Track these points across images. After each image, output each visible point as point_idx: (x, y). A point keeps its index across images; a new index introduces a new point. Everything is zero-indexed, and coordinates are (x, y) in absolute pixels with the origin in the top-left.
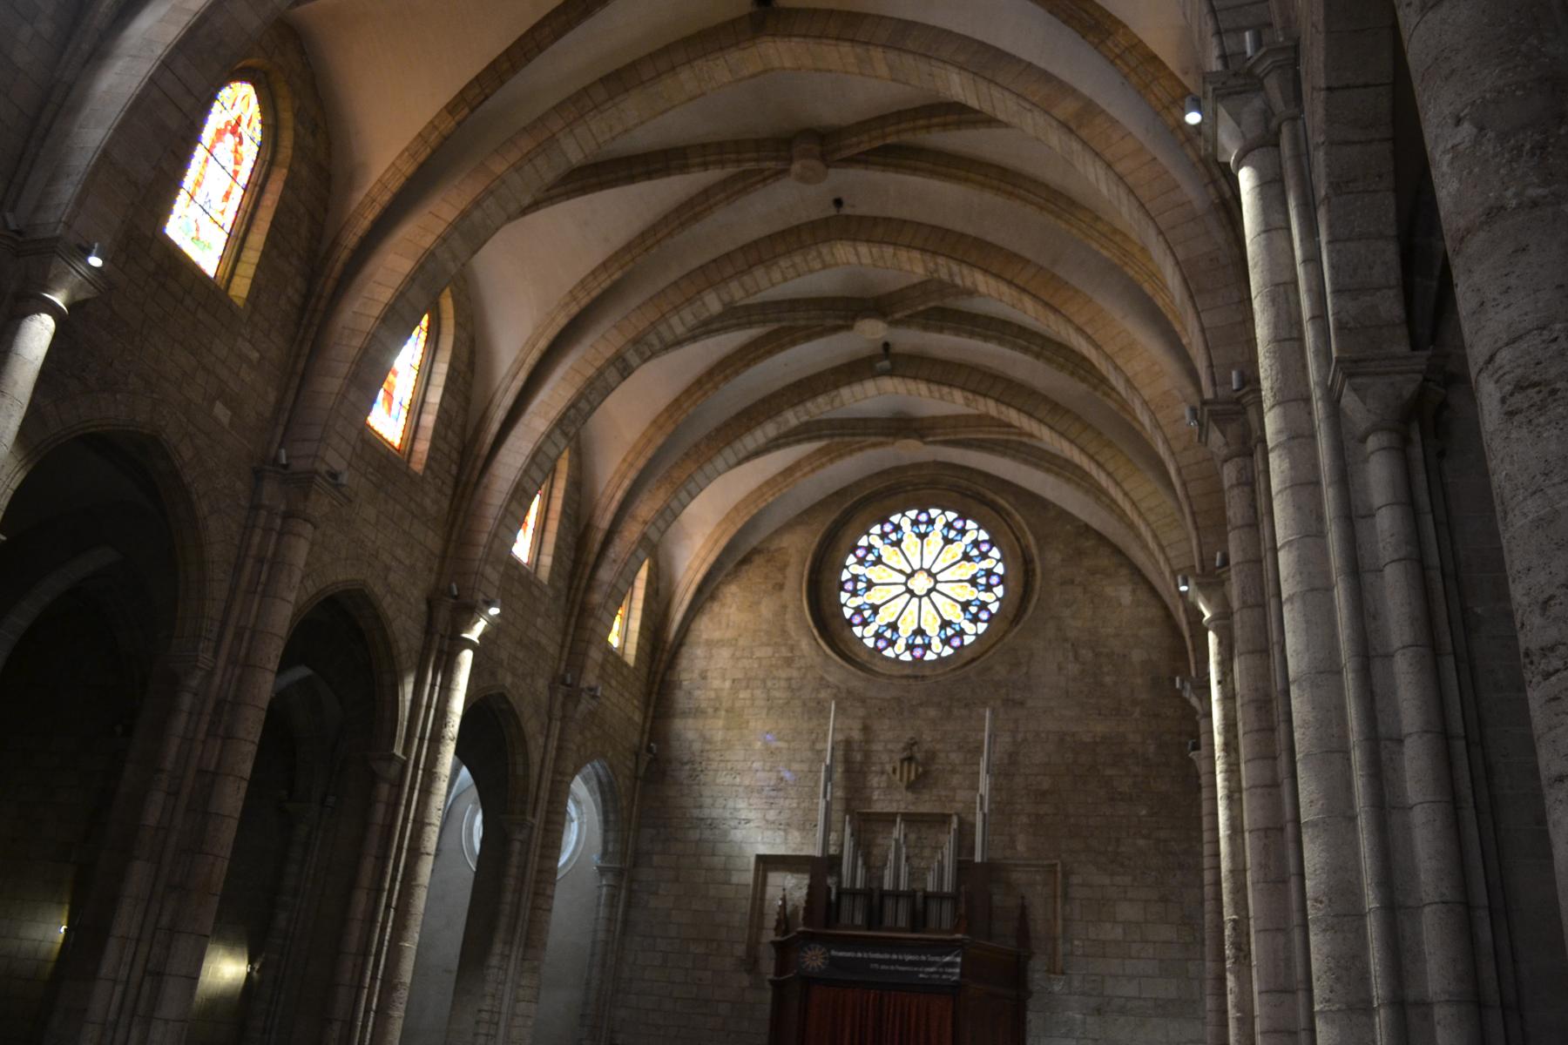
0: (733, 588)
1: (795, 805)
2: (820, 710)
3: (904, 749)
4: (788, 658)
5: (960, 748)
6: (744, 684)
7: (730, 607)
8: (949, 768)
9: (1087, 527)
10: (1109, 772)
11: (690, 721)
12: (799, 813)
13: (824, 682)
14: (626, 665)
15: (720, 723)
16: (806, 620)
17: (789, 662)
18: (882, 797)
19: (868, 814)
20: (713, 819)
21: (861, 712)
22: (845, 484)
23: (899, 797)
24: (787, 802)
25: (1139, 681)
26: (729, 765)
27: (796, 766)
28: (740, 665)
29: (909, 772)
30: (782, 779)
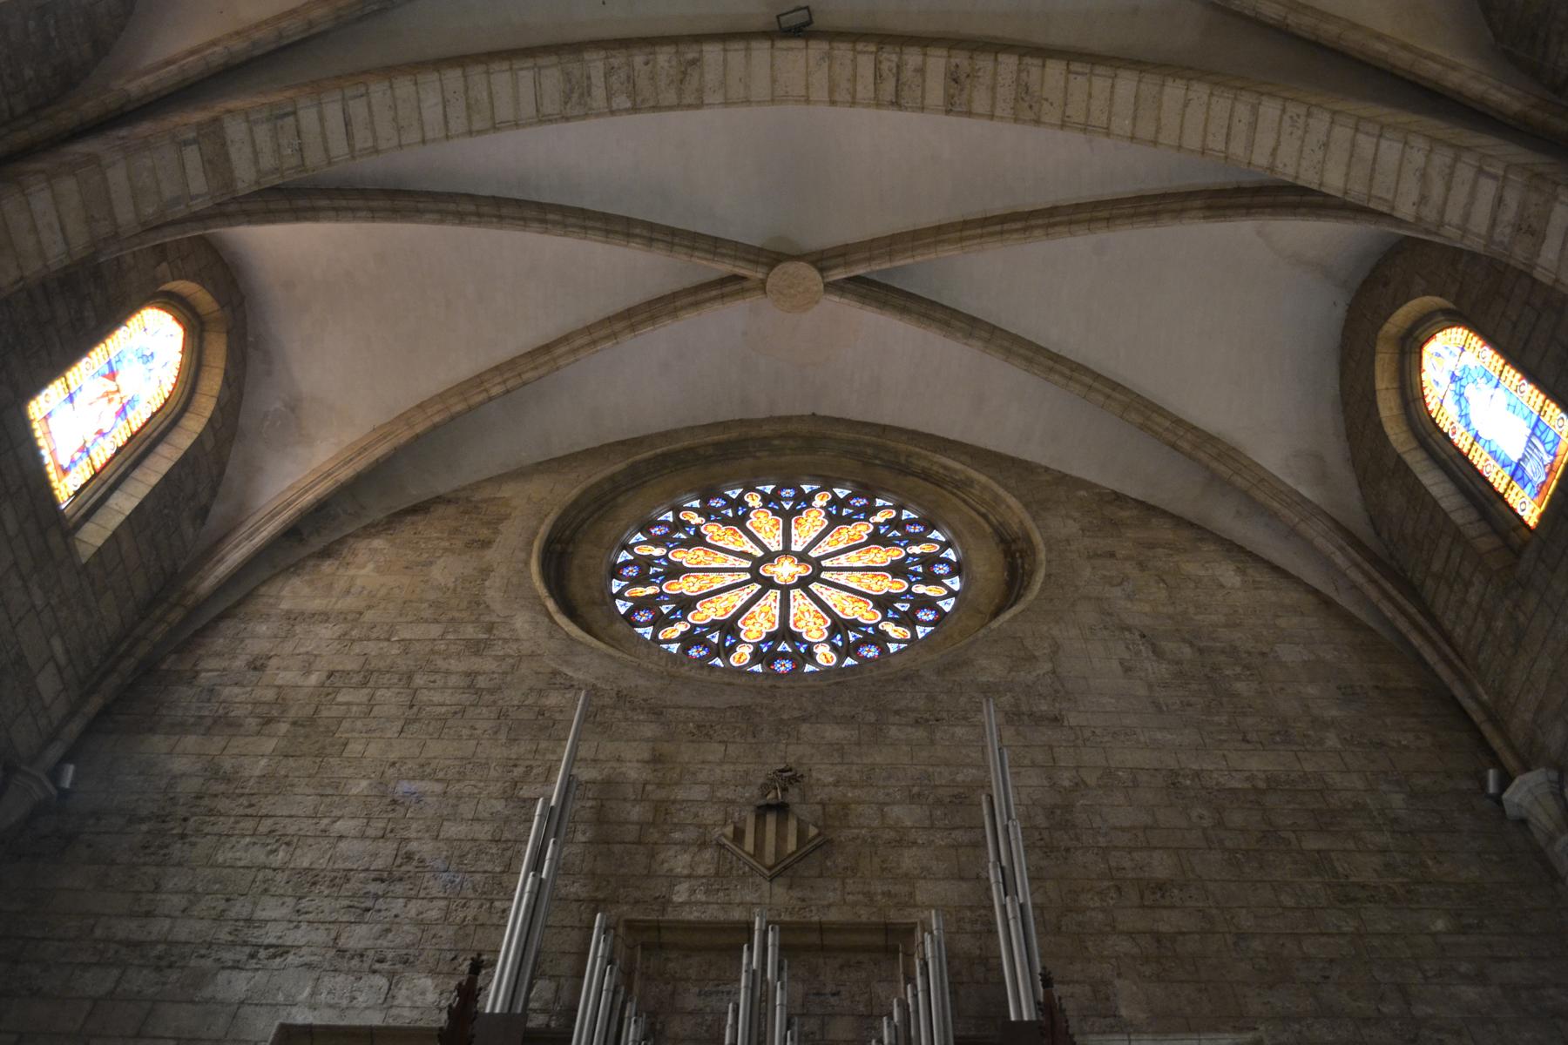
0: (378, 543)
1: (434, 914)
2: (546, 725)
3: (765, 788)
4: (479, 641)
5: (914, 798)
6: (356, 679)
7: (364, 566)
8: (889, 835)
9: (1118, 498)
10: (1312, 843)
11: (190, 742)
12: (448, 932)
13: (559, 680)
14: (71, 550)
15: (269, 745)
16: (532, 589)
17: (476, 648)
18: (700, 897)
19: (658, 927)
20: (172, 944)
21: (649, 730)
22: (641, 433)
23: (750, 897)
24: (414, 908)
25: (1311, 690)
26: (266, 825)
27: (452, 830)
28: (357, 648)
29: (781, 838)
30: (409, 857)
